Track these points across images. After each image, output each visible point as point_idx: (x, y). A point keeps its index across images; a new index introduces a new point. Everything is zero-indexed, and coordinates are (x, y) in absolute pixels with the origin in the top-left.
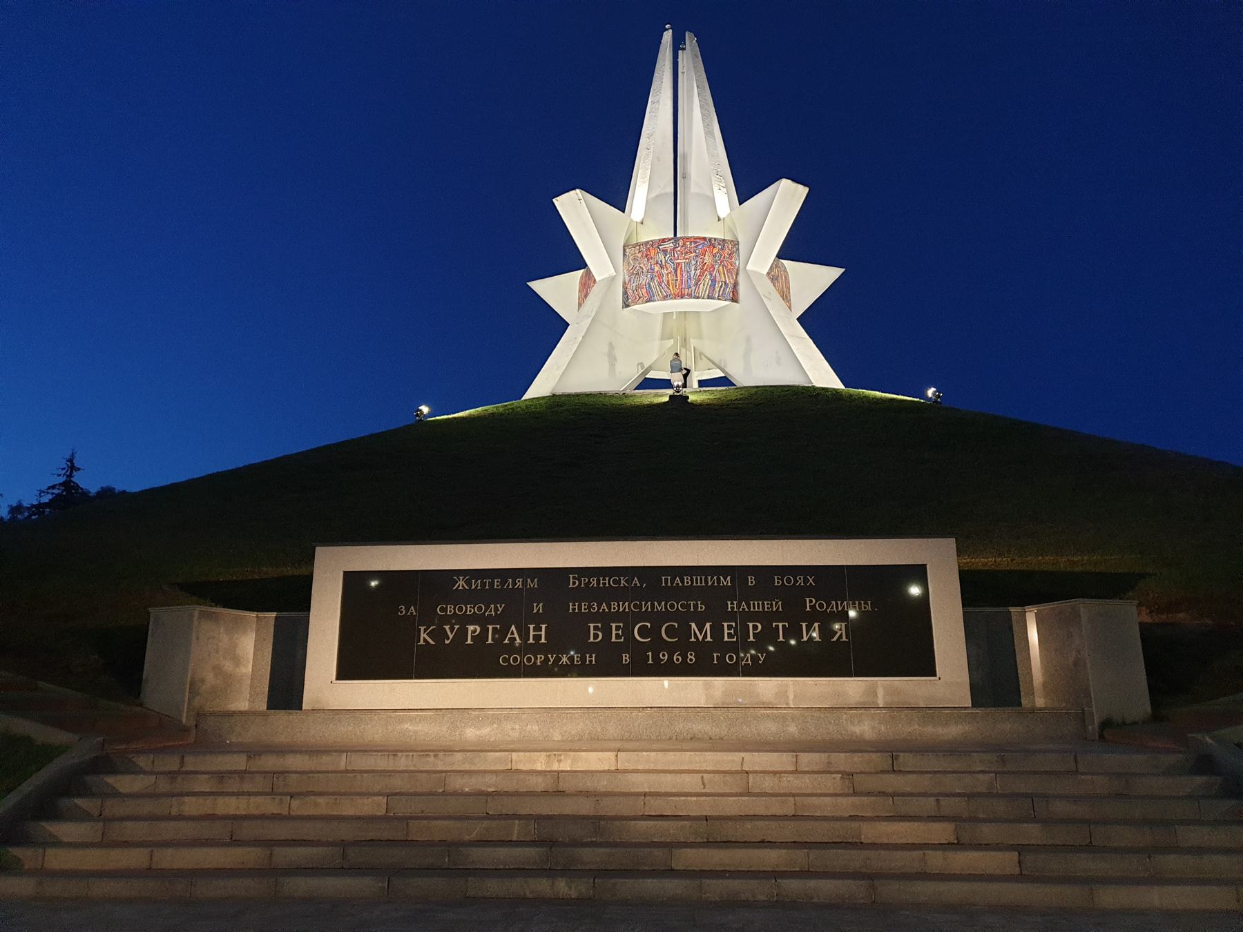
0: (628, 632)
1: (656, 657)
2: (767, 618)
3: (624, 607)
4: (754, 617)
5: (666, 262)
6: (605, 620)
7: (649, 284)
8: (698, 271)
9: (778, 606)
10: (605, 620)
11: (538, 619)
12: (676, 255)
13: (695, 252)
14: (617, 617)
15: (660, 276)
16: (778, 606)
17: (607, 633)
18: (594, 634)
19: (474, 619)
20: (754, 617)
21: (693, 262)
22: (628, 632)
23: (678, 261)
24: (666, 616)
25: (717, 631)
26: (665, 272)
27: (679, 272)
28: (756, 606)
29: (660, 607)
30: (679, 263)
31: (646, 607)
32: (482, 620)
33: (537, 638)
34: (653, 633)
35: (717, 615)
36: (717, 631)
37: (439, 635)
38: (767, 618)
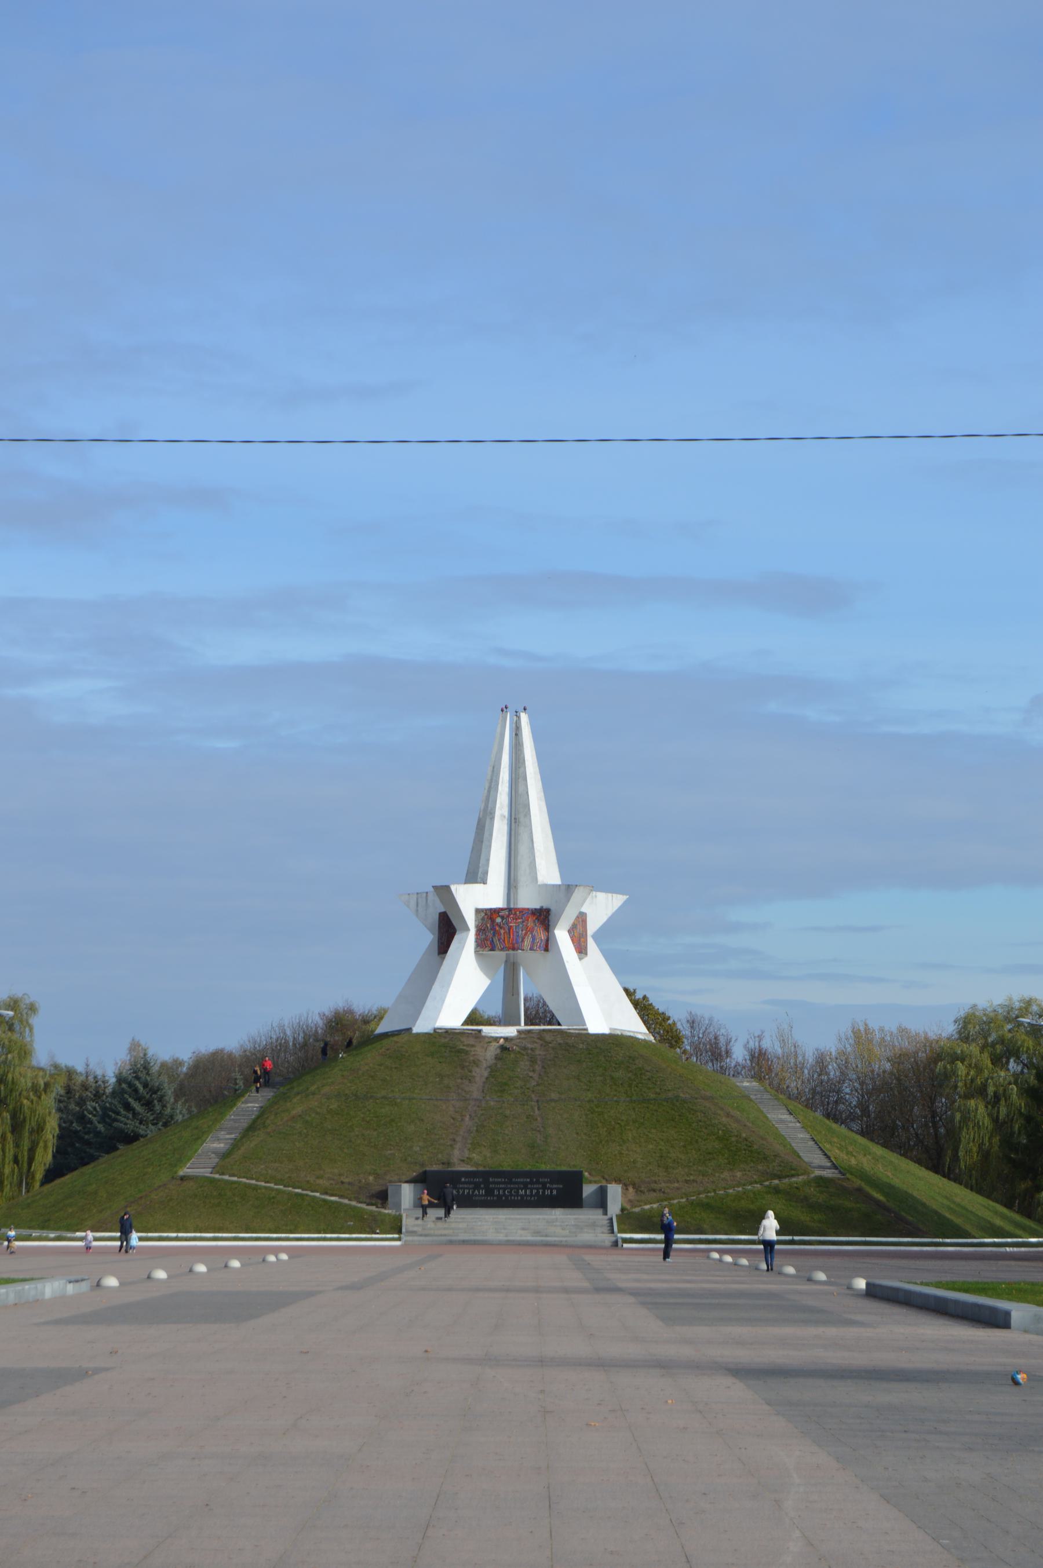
0: (504, 1192)
1: (511, 1198)
2: (538, 1189)
3: (503, 1186)
4: (534, 1188)
5: (503, 924)
6: (499, 1189)
7: (492, 939)
8: (524, 932)
9: (541, 1186)
10: (499, 1189)
11: (482, 1189)
12: (510, 920)
13: (522, 918)
14: (501, 1188)
15: (500, 934)
16: (541, 1186)
17: (499, 1193)
18: (496, 1192)
19: (466, 1188)
20: (534, 1188)
21: (521, 926)
22: (504, 1192)
23: (511, 925)
24: (514, 1188)
25: (526, 1192)
26: (502, 931)
27: (511, 931)
28: (535, 1186)
29: (512, 1186)
30: (511, 926)
31: (509, 1186)
32: (469, 1189)
33: (482, 1193)
34: (511, 1192)
35: (526, 1188)
36: (526, 1192)
37: (458, 1192)
38: (538, 1189)
